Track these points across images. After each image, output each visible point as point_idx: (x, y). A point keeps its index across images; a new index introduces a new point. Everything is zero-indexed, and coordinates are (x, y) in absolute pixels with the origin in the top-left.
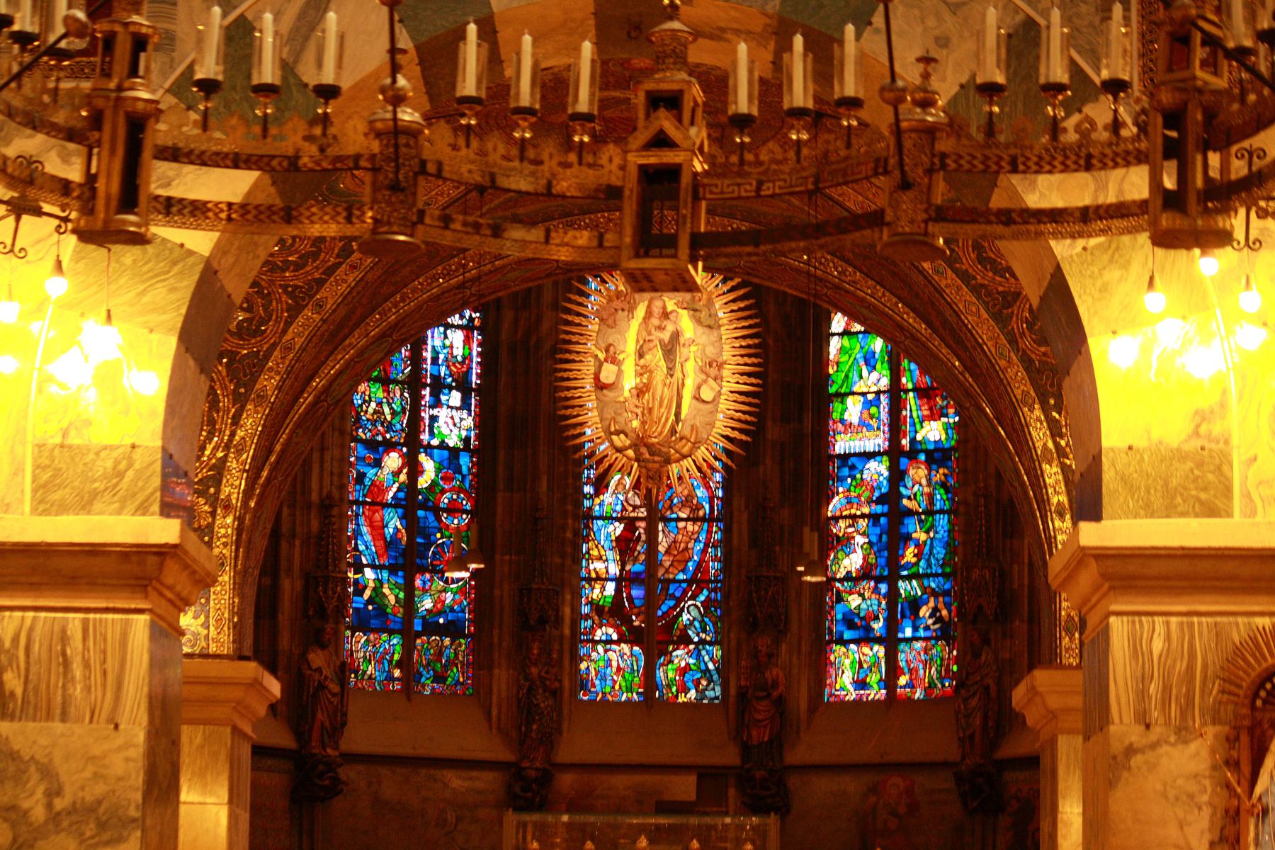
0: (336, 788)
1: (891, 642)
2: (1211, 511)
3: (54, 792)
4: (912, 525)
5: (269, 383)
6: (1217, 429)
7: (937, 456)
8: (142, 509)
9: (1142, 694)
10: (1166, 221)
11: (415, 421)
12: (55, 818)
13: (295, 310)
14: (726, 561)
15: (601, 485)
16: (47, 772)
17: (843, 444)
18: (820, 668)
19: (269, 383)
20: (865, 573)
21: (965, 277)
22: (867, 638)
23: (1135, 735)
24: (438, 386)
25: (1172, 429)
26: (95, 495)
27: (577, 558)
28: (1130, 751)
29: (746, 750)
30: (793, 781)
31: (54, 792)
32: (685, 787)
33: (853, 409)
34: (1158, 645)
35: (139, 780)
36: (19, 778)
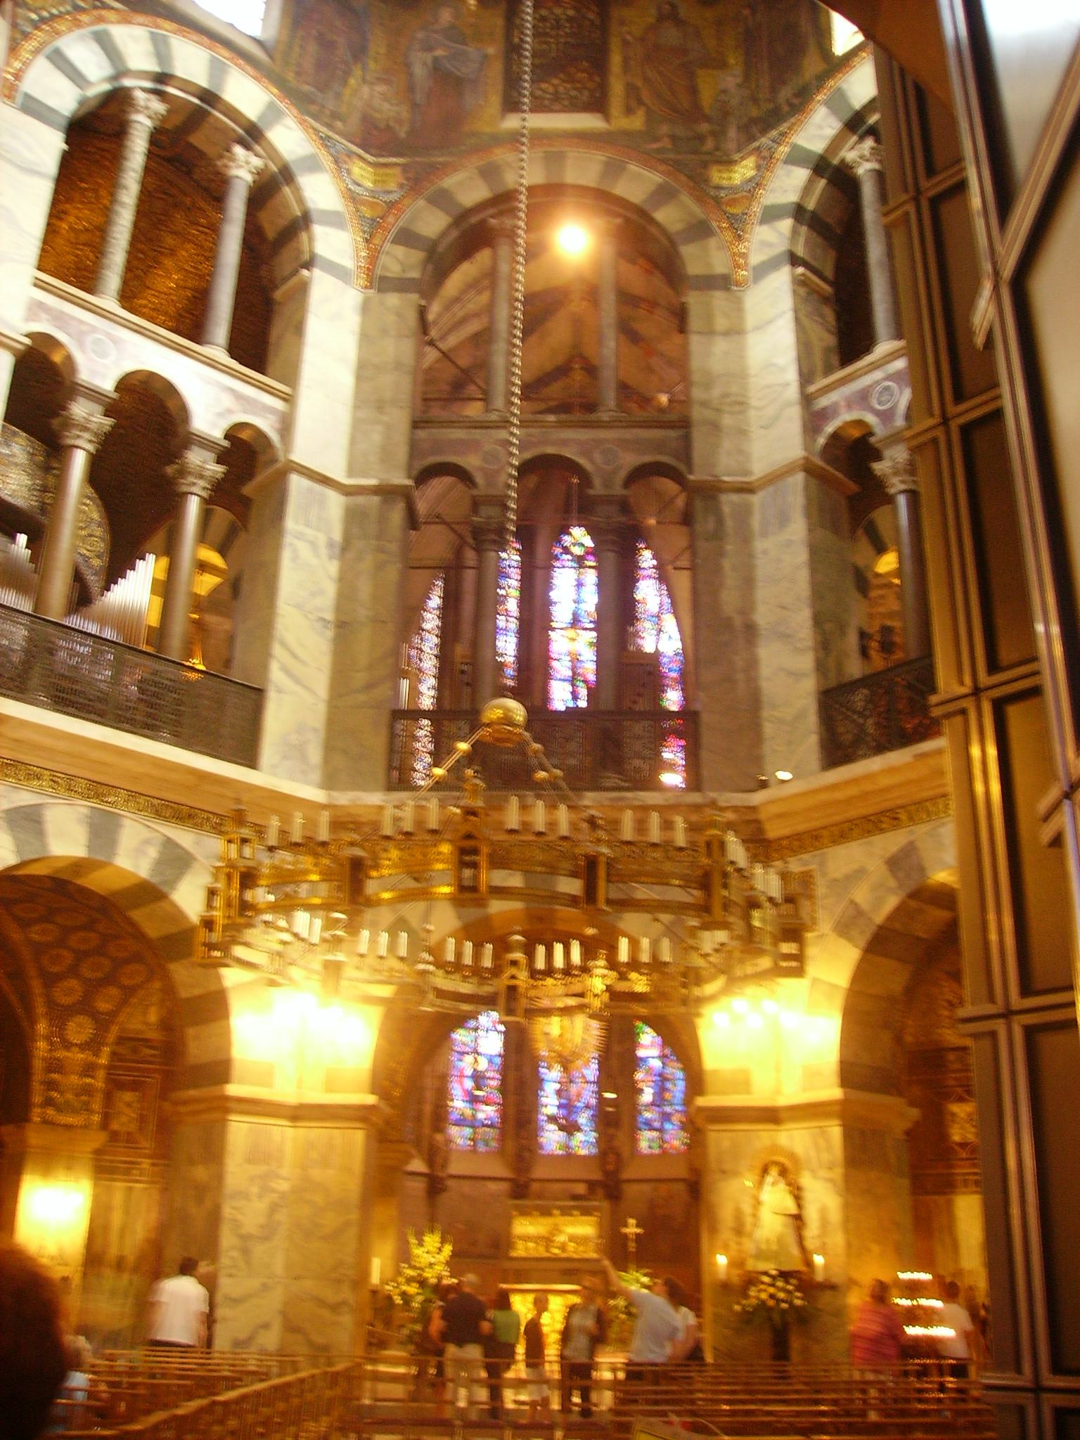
1: (661, 1130)
4: (669, 1085)
18: (634, 1141)
20: (653, 1104)
22: (652, 1129)
27: (537, 1096)
29: (606, 1173)
30: (625, 1187)
32: (581, 1189)
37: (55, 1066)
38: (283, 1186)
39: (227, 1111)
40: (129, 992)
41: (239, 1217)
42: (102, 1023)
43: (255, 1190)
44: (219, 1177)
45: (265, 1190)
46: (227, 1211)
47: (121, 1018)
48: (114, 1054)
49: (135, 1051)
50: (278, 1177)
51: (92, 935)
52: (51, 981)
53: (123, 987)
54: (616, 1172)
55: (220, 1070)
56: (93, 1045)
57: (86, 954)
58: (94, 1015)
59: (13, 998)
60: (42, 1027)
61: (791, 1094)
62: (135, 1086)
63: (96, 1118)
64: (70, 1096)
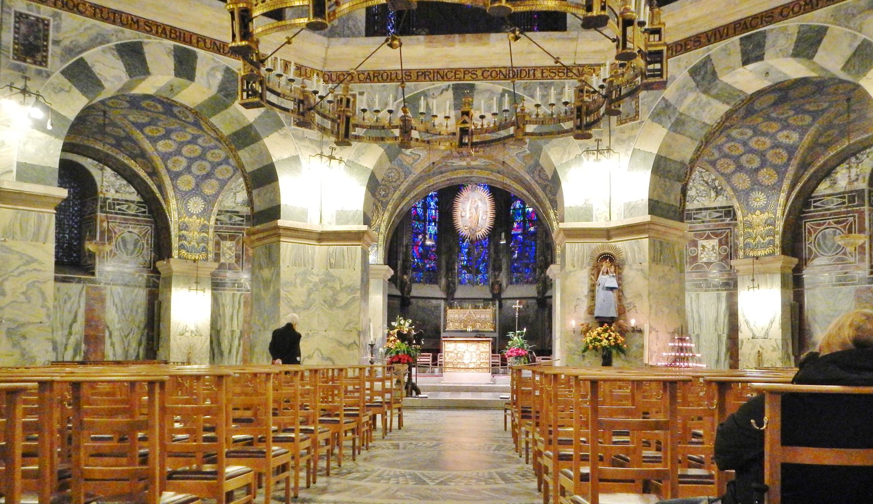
0: (410, 303)
2: (589, 219)
3: (341, 283)
5: (390, 207)
6: (590, 202)
7: (534, 234)
8: (359, 224)
9: (573, 260)
10: (576, 132)
11: (425, 228)
12: (342, 289)
13: (395, 191)
14: (489, 257)
15: (463, 241)
16: (340, 280)
17: (513, 232)
19: (390, 207)
21: (536, 181)
23: (571, 268)
24: (430, 222)
25: (580, 204)
26: (349, 221)
28: (570, 272)
29: (493, 295)
31: (341, 283)
33: (515, 225)
34: (576, 249)
35: (360, 280)
36: (334, 281)
37: (184, 227)
38: (316, 279)
39: (279, 236)
40: (223, 184)
41: (290, 296)
42: (209, 201)
43: (298, 281)
44: (278, 274)
45: (304, 281)
46: (282, 293)
47: (220, 198)
48: (217, 220)
49: (231, 218)
50: (313, 274)
51: (197, 147)
52: (174, 176)
53: (218, 179)
54: (500, 293)
55: (274, 212)
56: (206, 213)
57: (195, 159)
58: (205, 198)
59: (154, 188)
60: (173, 204)
61: (618, 221)
62: (232, 238)
63: (211, 256)
64: (194, 243)
